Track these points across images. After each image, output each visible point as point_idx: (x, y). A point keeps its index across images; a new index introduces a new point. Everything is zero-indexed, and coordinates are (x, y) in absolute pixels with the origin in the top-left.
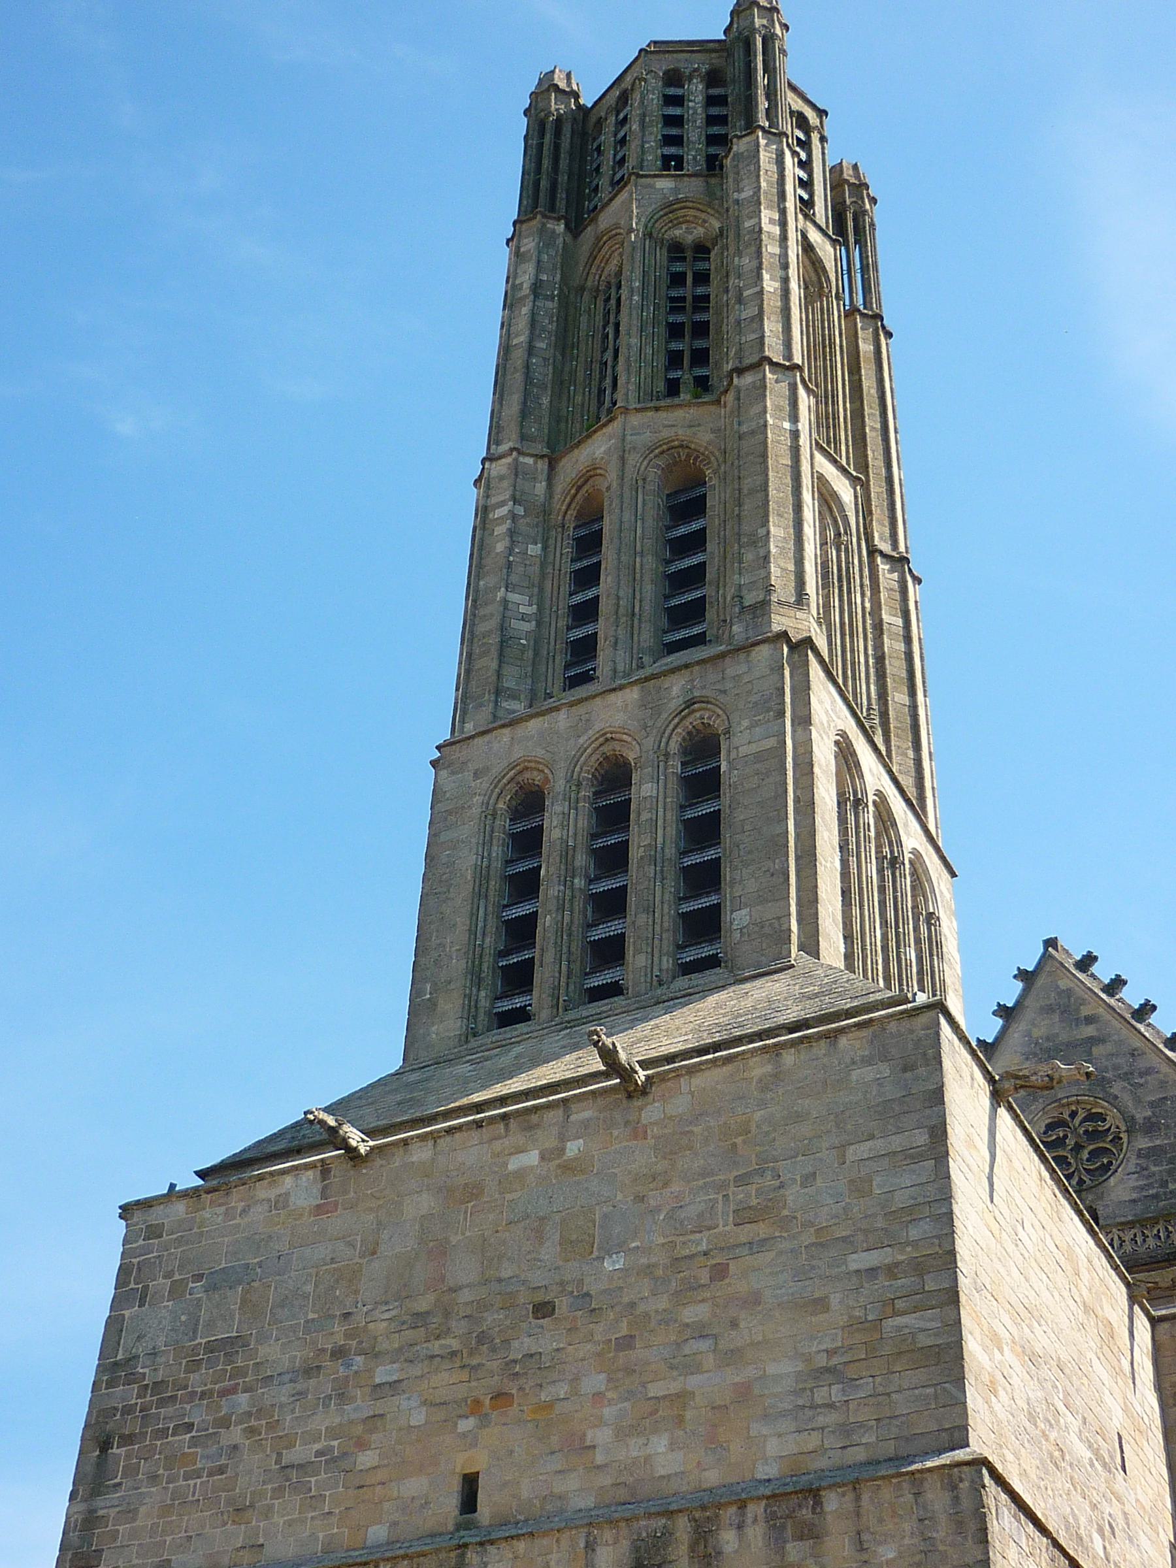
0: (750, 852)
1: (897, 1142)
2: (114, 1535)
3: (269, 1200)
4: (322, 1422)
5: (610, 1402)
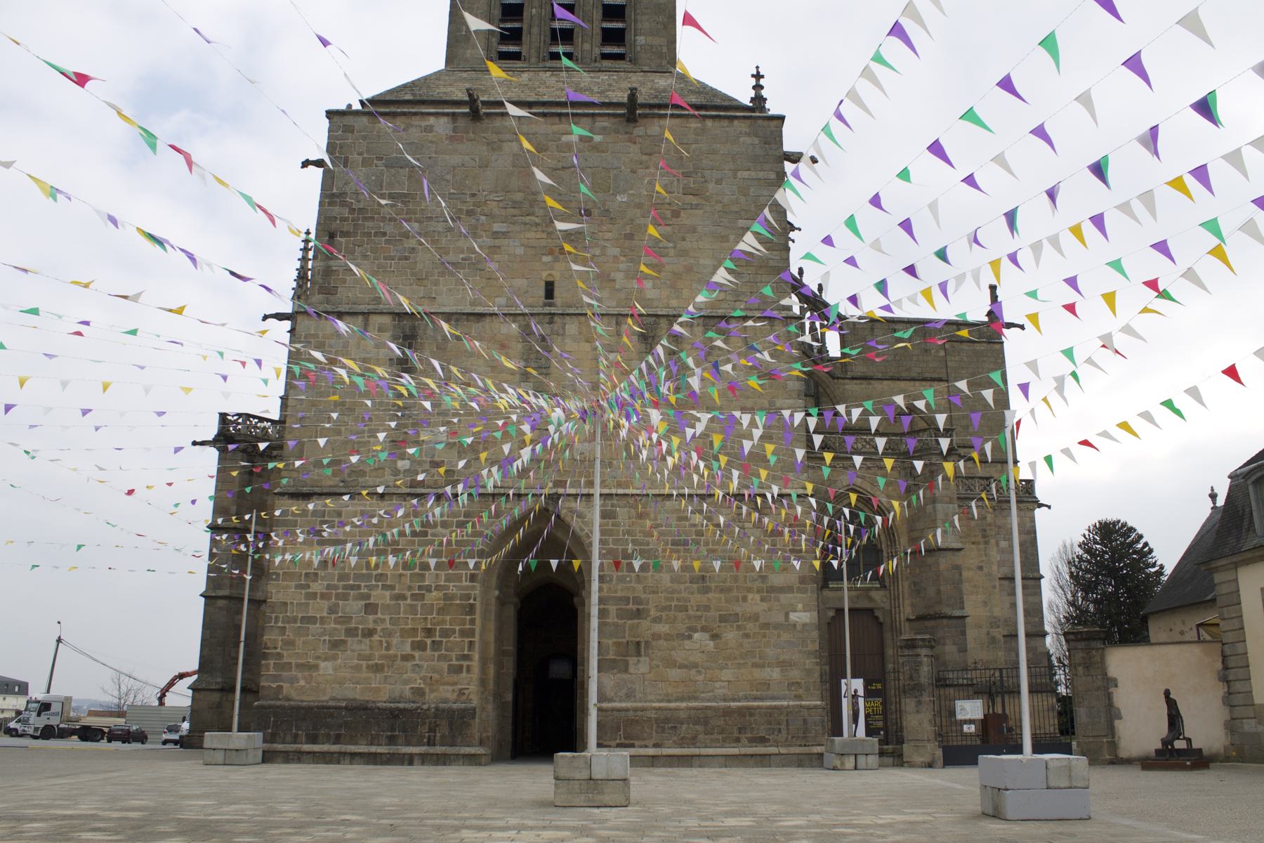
0: (646, 8)
1: (761, 175)
2: (344, 281)
3: (421, 126)
5: (622, 262)
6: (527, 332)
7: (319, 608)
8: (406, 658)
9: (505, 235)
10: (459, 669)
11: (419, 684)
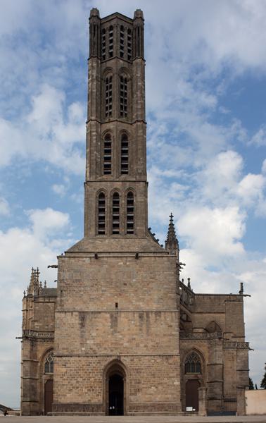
4: (95, 293)
6: (112, 316)
7: (66, 382)
8: (86, 393)
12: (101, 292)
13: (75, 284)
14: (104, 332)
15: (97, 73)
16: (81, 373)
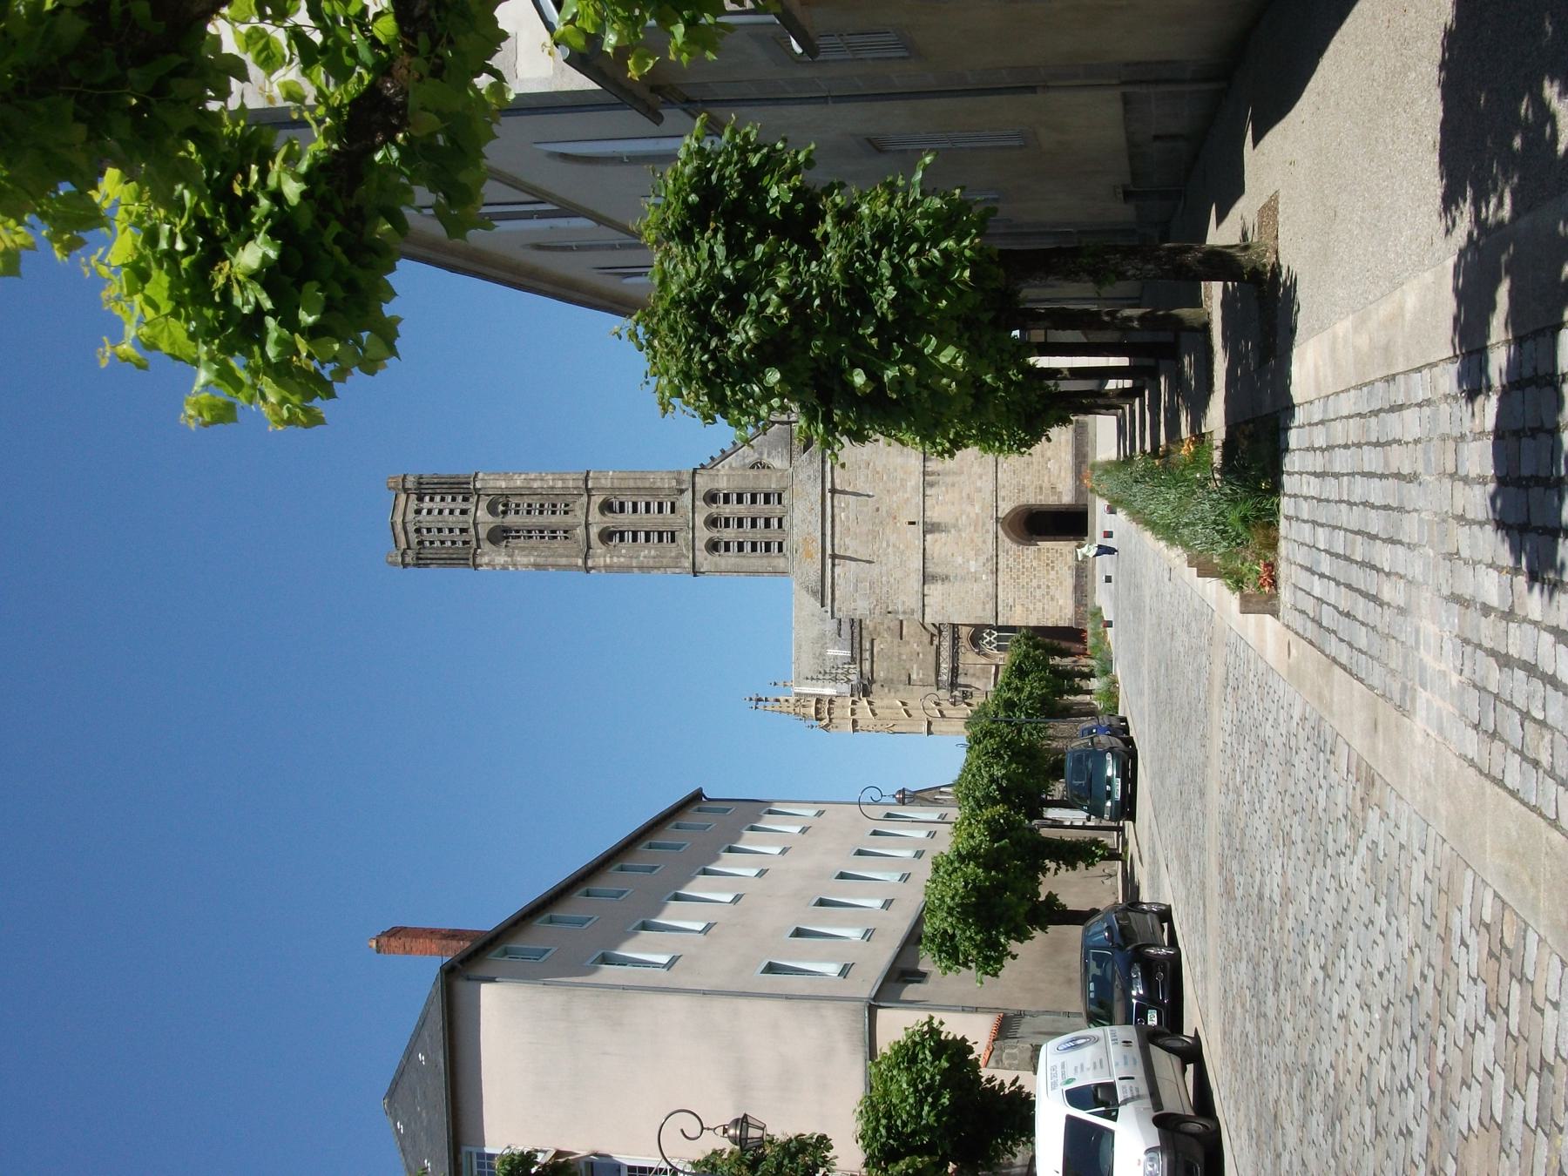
4: (891, 558)
7: (1039, 606)
8: (1057, 573)
9: (888, 542)
10: (1061, 553)
11: (1066, 568)
12: (890, 550)
13: (878, 591)
14: (957, 543)
15: (500, 555)
16: (1023, 580)
